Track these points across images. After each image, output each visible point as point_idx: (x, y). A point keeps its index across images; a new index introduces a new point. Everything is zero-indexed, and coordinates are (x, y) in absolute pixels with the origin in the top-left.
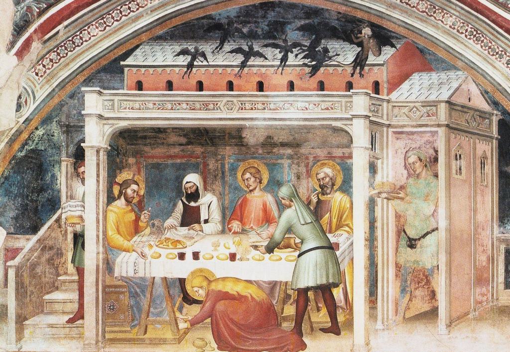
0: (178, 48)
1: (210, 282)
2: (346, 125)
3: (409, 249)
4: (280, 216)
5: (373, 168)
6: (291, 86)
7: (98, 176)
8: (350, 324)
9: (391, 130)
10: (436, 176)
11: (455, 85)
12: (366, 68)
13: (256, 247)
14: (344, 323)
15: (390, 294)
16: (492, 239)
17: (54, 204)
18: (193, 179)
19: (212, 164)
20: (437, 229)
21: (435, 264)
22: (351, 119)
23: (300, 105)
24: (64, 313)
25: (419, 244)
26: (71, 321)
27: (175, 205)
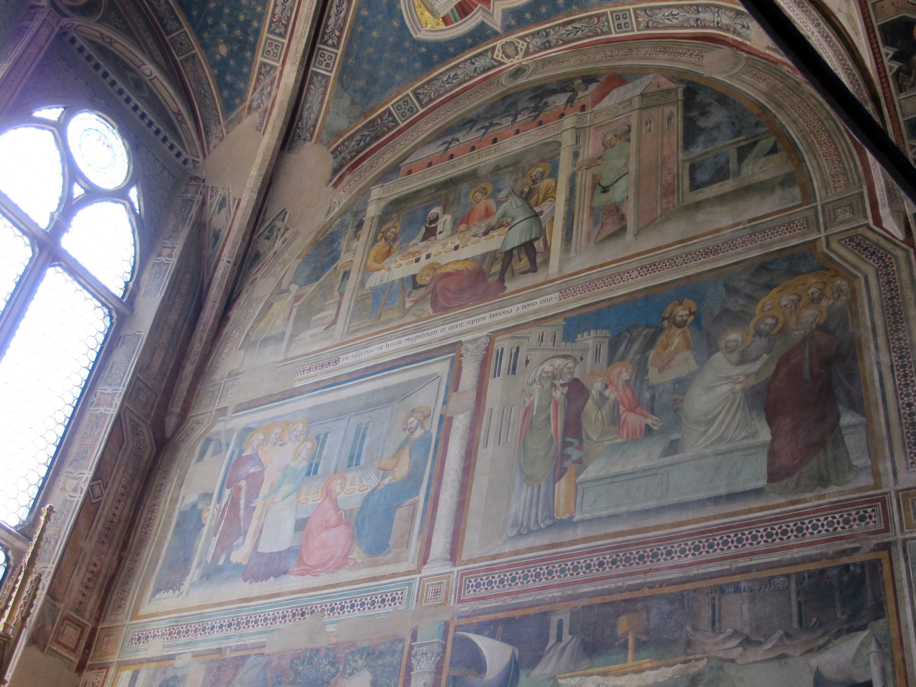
0: (440, 143)
1: (435, 269)
3: (603, 194)
4: (497, 209)
6: (518, 132)
7: (369, 232)
8: (546, 262)
9: (592, 128)
10: (629, 140)
11: (647, 83)
12: (576, 101)
13: (475, 236)
14: (541, 263)
15: (584, 230)
16: (678, 162)
17: (335, 259)
19: (451, 198)
20: (628, 173)
21: (625, 196)
22: (561, 133)
23: (522, 140)
24: (324, 324)
25: (611, 189)
26: (327, 328)
27: (420, 230)
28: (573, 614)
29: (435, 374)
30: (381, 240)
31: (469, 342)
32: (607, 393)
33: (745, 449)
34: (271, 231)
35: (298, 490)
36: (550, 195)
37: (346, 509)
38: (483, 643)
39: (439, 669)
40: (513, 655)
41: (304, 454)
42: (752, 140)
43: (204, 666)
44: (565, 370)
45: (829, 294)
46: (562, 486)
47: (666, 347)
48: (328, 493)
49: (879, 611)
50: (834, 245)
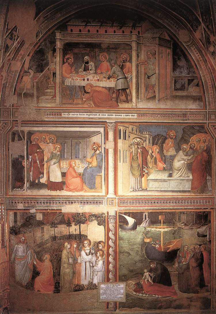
2: (130, 43)
5: (138, 56)
18: (86, 58)
28: (148, 213)
29: (100, 132)
30: (66, 63)
31: (109, 123)
32: (153, 154)
33: (187, 180)
34: (12, 35)
35: (59, 162)
36: (130, 71)
37: (78, 172)
38: (127, 217)
39: (116, 223)
40: (135, 221)
41: (58, 149)
42: (192, 78)
43: (42, 214)
44: (141, 143)
45: (207, 141)
46: (143, 179)
47: (168, 145)
48: (71, 166)
49: (210, 222)
50: (210, 127)
